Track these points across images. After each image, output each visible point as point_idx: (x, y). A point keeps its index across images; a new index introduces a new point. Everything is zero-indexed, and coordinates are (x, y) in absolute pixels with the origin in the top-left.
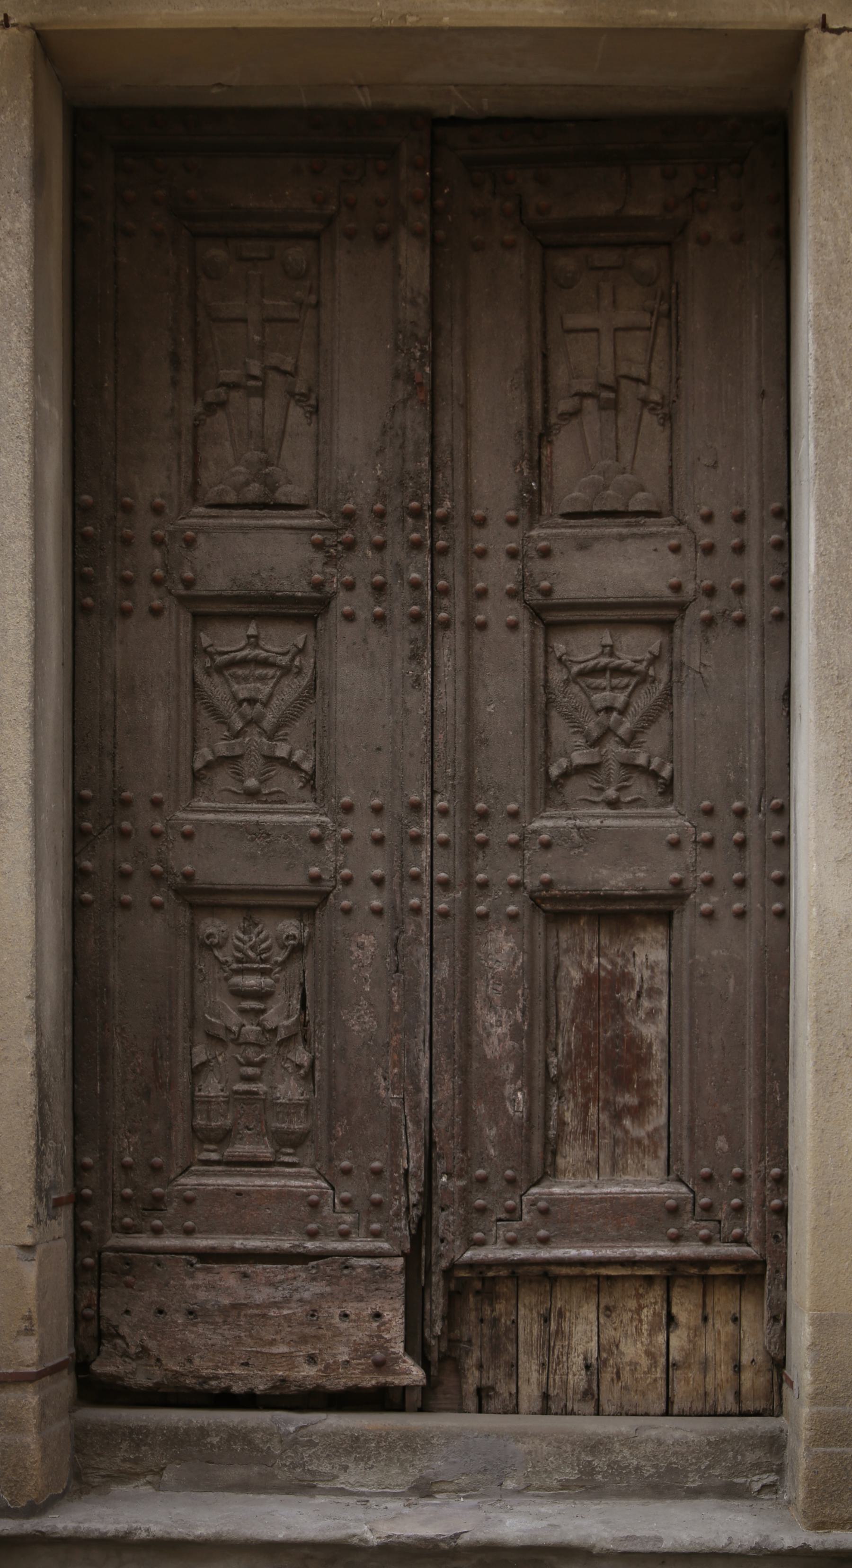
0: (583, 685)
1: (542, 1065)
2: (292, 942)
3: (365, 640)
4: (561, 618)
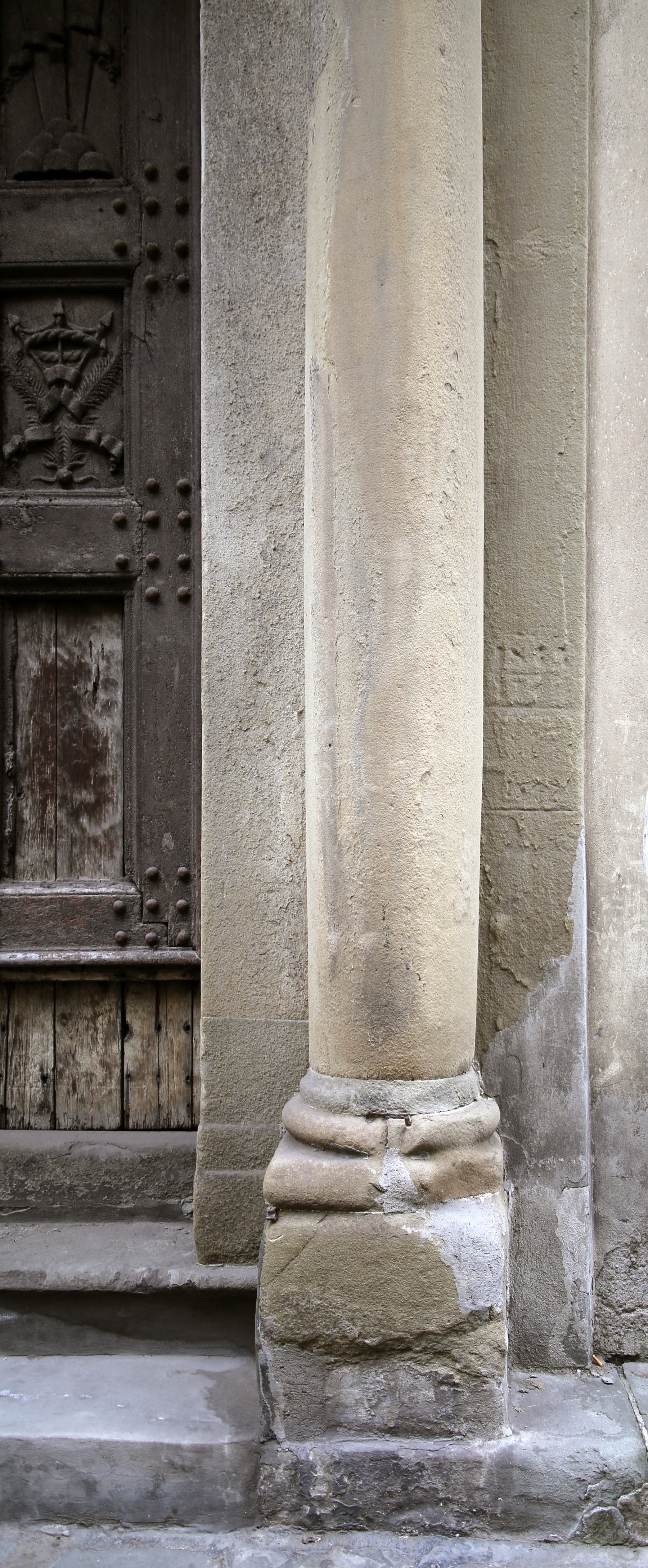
0: (35, 357)
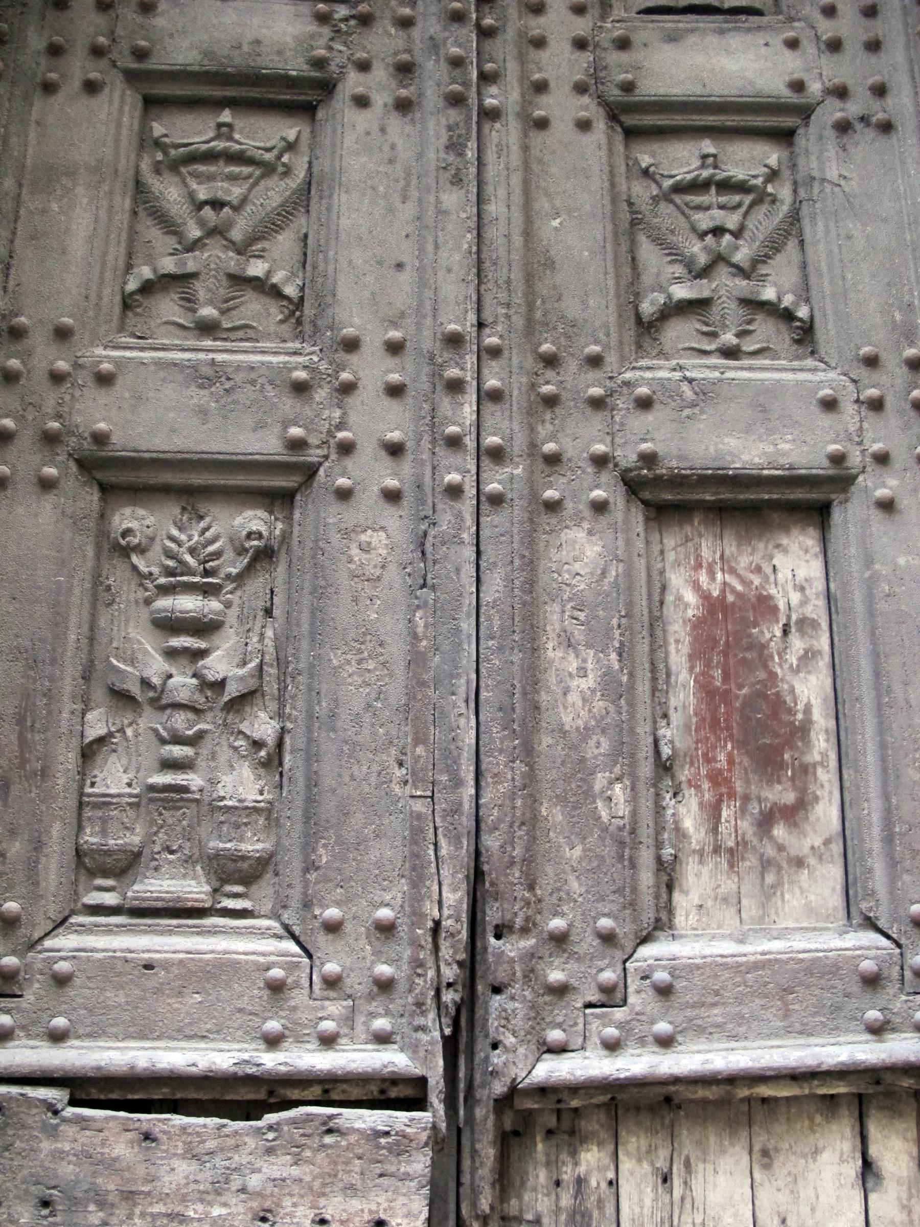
1: (650, 740)
2: (256, 543)
3: (383, 130)
4: (646, 122)
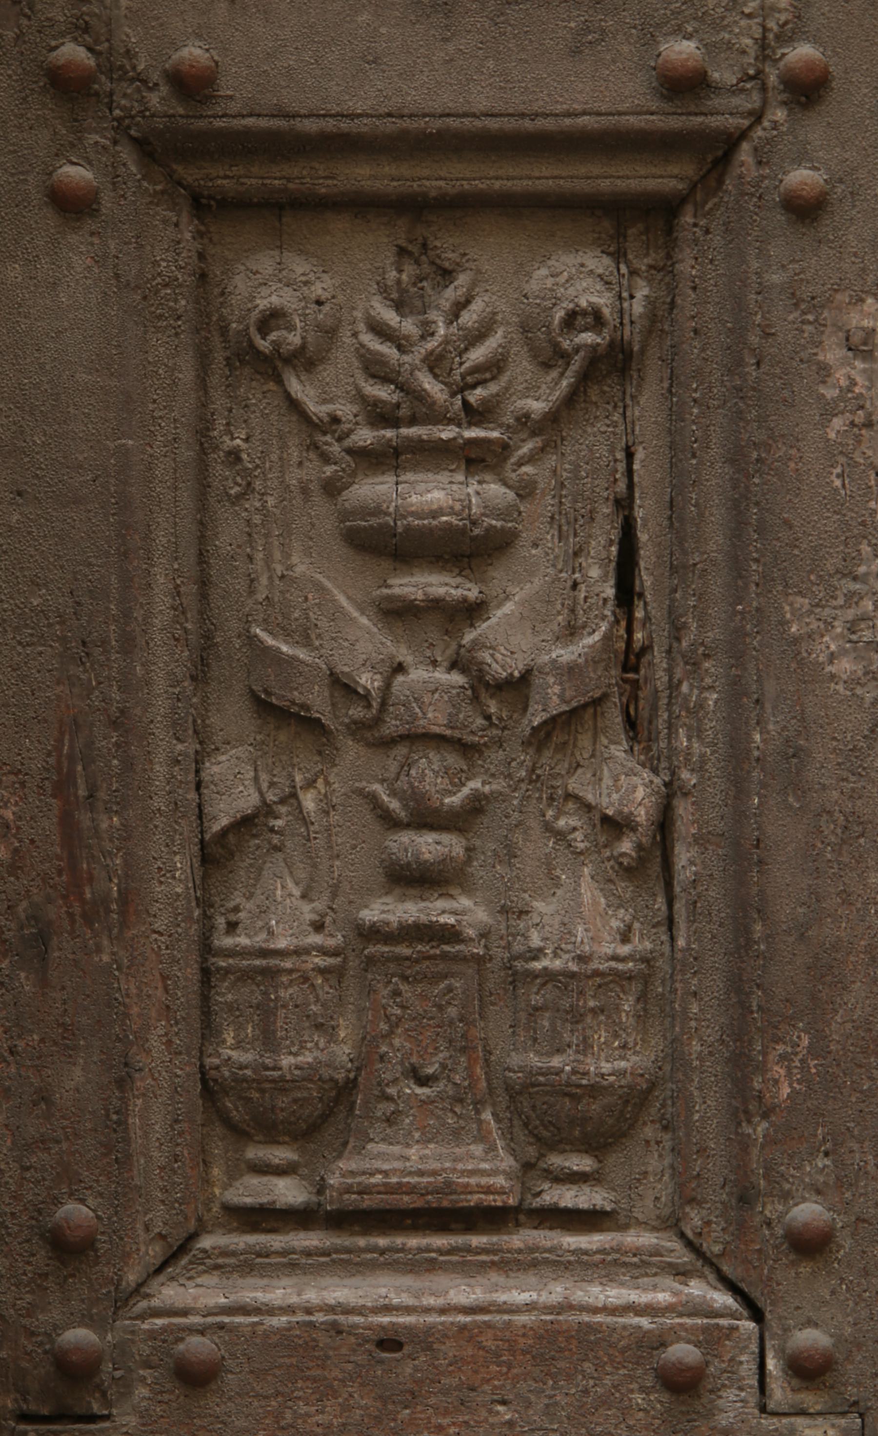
2: (588, 338)
